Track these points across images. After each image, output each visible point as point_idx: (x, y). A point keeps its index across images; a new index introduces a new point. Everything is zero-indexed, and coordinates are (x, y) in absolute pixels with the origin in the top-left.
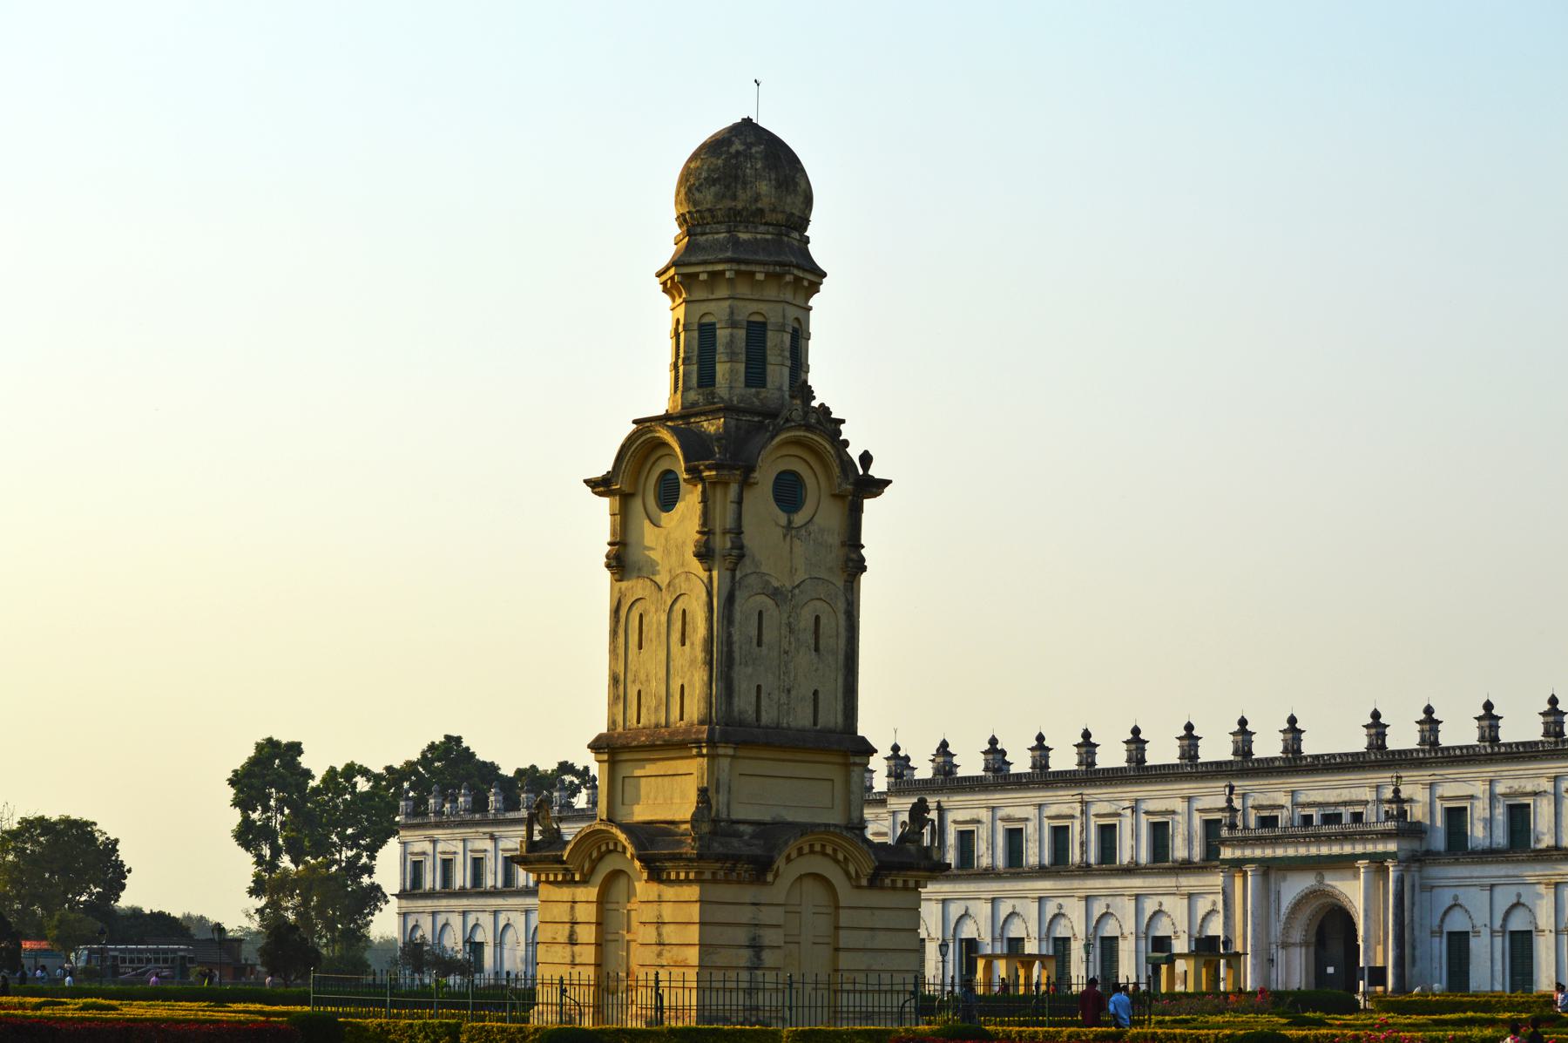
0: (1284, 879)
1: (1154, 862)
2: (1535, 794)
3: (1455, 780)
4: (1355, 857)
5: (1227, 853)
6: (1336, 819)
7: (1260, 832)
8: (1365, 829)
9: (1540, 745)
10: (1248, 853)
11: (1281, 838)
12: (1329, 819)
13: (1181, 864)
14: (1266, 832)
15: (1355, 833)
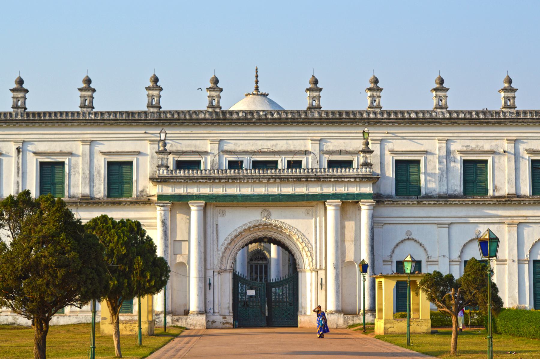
0: (223, 214)
1: (109, 196)
2: (492, 152)
3: (403, 138)
4: (323, 198)
5: (168, 190)
6: (297, 164)
7: (256, 173)
8: (335, 174)
9: (501, 114)
10: (193, 190)
11: (173, 179)
12: (295, 164)
13: (81, 199)
14: (232, 173)
15: (331, 177)
